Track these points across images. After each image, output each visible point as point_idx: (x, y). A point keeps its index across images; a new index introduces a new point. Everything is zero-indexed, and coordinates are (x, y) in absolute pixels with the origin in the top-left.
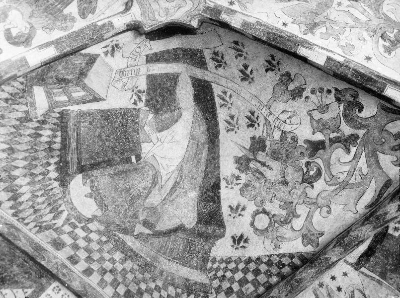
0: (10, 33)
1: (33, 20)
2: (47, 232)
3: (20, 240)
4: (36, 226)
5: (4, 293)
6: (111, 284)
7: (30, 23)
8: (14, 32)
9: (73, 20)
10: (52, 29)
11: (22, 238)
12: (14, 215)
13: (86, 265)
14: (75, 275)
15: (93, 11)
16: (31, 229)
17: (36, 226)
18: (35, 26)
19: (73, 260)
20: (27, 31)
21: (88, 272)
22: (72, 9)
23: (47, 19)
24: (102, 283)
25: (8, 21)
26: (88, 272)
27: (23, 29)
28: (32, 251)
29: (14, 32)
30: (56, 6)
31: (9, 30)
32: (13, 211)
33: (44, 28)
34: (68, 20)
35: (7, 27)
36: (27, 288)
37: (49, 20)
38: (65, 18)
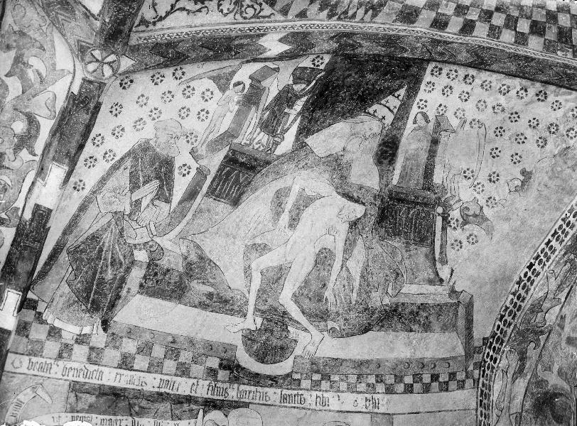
2: (386, 9)
3: (361, 46)
4: (366, 12)
5: (372, 113)
6: (507, 26)
11: (362, 42)
12: (330, 17)
13: (461, 20)
14: (455, 45)
16: (362, 19)
17: (366, 12)
19: (440, 24)
21: (468, 28)
24: (494, 32)
26: (468, 28)
28: (384, 49)
32: (326, 12)
36: (397, 90)
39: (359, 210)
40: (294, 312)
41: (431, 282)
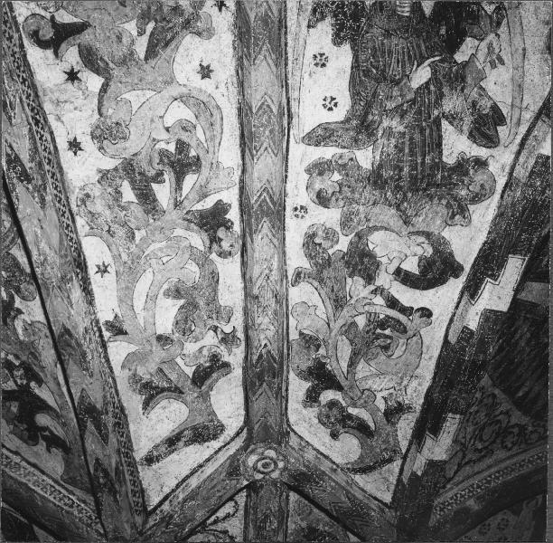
0: (407, 274)
1: (420, 223)
7: (418, 233)
8: (412, 266)
9: (481, 164)
10: (463, 210)
18: (434, 229)
20: (430, 251)
22: (456, 144)
23: (436, 201)
25: (384, 260)
27: (419, 251)
29: (412, 266)
30: (423, 162)
31: (398, 272)
34: (471, 172)
35: (392, 269)
37: (440, 199)
38: (462, 167)
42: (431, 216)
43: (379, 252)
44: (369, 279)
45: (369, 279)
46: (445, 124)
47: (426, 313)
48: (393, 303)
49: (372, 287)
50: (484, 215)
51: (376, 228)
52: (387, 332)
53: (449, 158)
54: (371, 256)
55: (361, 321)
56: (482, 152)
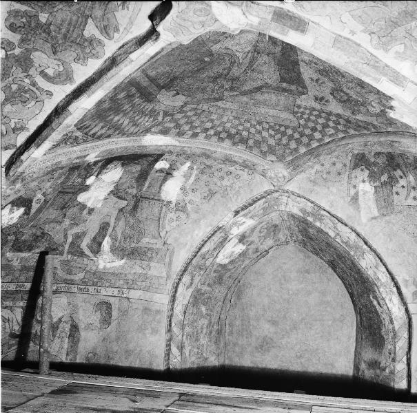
15: (117, 29)
22: (91, 30)
25: (37, 65)
29: (50, 72)
33: (77, 60)
39: (123, 203)
40: (87, 252)
41: (154, 237)
42: (69, 55)
43: (35, 60)
44: (26, 70)
45: (26, 70)
46: (90, 21)
47: (50, 94)
48: (34, 84)
49: (26, 74)
50: (94, 65)
51: (37, 50)
52: (27, 95)
53: (87, 34)
54: (31, 61)
55: (14, 87)
56: (102, 38)
